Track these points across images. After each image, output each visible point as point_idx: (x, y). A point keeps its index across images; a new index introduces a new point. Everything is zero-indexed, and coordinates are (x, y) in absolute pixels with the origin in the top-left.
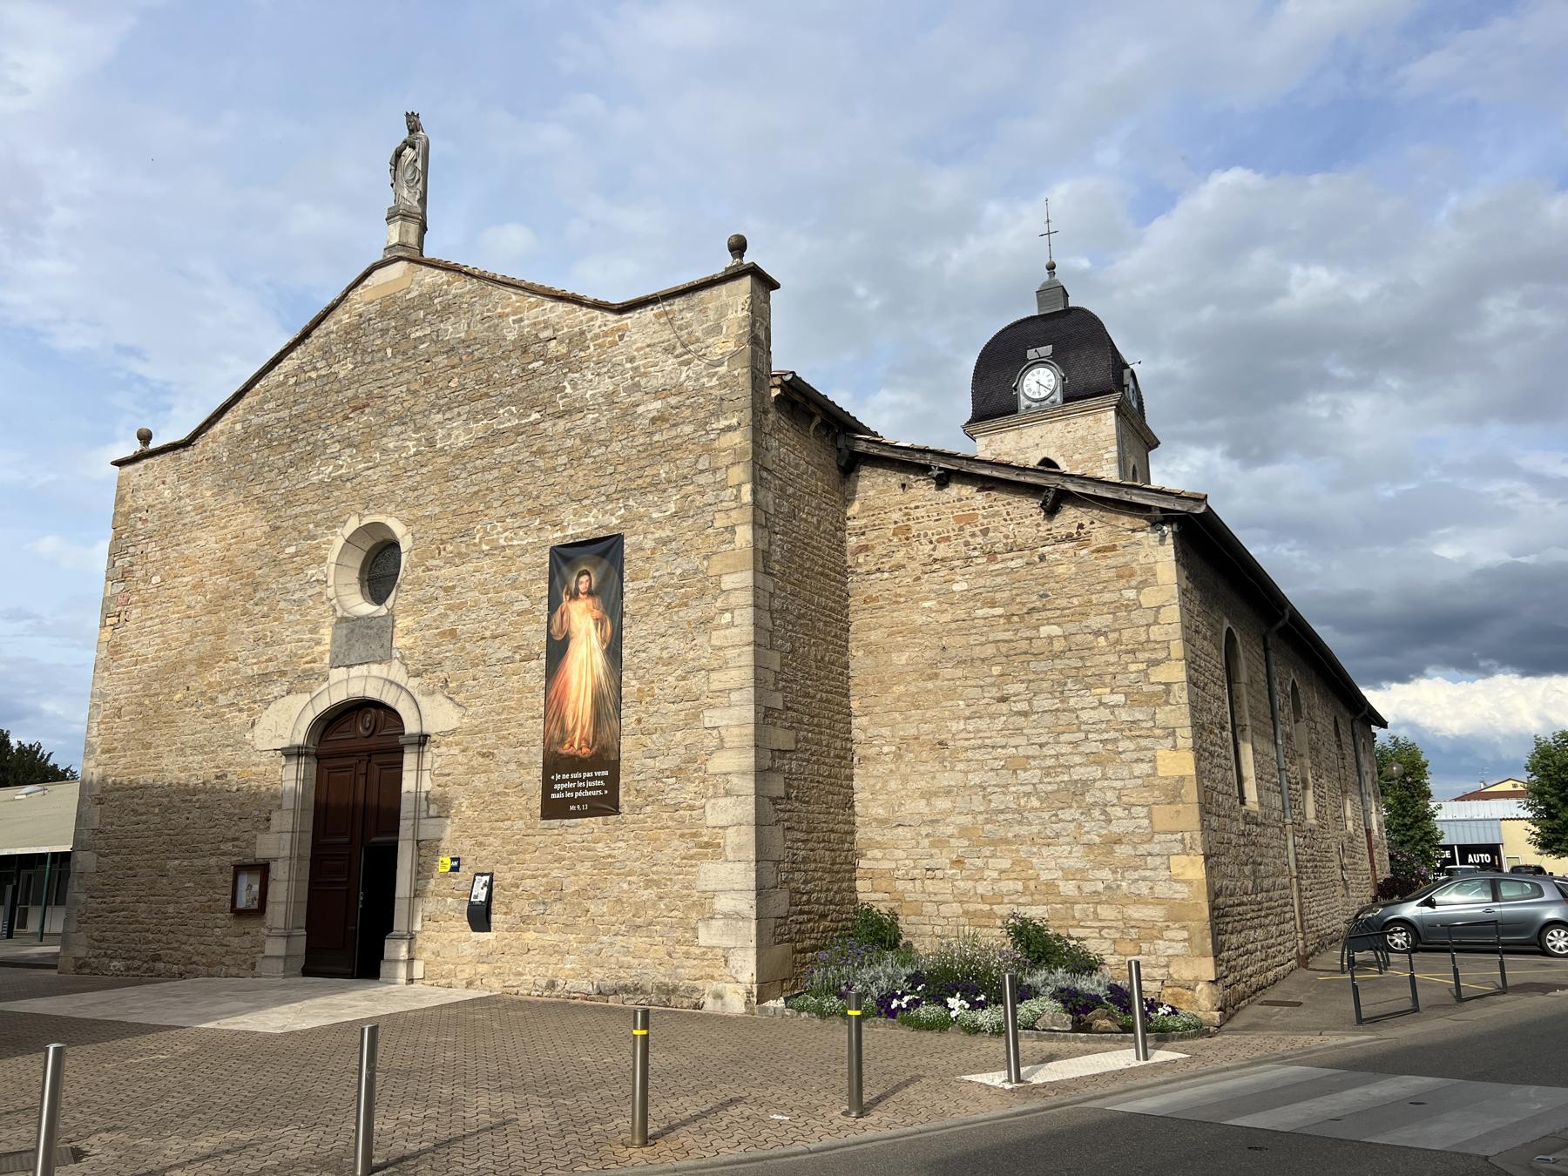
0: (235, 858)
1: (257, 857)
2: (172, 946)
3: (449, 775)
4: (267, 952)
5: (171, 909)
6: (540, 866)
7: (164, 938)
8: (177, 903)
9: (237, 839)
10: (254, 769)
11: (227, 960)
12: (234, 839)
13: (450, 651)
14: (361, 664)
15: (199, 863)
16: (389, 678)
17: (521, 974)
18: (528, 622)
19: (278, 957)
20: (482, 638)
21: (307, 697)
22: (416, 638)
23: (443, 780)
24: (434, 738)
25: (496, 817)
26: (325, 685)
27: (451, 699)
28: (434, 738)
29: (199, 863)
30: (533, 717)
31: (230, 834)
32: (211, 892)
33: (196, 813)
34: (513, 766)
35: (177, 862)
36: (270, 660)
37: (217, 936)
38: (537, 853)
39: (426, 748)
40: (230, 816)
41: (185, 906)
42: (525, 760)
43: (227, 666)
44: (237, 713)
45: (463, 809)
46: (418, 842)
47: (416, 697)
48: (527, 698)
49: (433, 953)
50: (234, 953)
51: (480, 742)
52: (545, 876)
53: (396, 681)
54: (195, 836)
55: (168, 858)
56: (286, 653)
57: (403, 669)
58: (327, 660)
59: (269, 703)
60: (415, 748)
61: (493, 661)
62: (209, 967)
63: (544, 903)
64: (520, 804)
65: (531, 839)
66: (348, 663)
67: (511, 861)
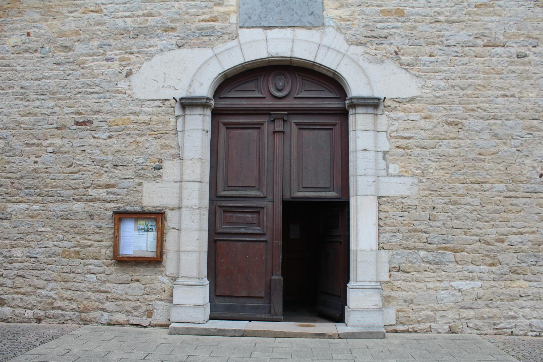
0: (112, 205)
1: (144, 205)
2: (22, 290)
3: (409, 138)
4: (176, 301)
5: (17, 253)
6: (526, 224)
7: (10, 283)
8: (26, 247)
9: (113, 186)
10: (132, 117)
11: (108, 305)
12: (108, 186)
13: (396, 28)
14: (282, 27)
15: (58, 208)
16: (323, 43)
17: (514, 318)
18: (488, 14)
19: (196, 306)
20: (437, 21)
21: (208, 52)
22: (354, 12)
23: (403, 142)
24: (387, 103)
25: (472, 180)
26: (234, 43)
27: (405, 69)
28: (387, 103)
29: (58, 208)
30: (505, 96)
31: (104, 180)
32: (78, 238)
33: (46, 157)
34: (486, 135)
35: (22, 206)
36: (150, 15)
37: (90, 282)
38: (522, 213)
39: (379, 112)
40: (101, 164)
41: (40, 250)
42: (500, 131)
43: (86, 16)
44: (105, 62)
45: (431, 171)
46: (379, 198)
47: (361, 63)
48: (495, 78)
49: (405, 301)
50: (117, 299)
51: (445, 112)
52: (533, 232)
53: (332, 46)
54: (48, 181)
55: (10, 201)
56: (173, 10)
57: (341, 37)
58: (233, 19)
59: (152, 55)
60: (370, 110)
61: (451, 42)
62: (82, 312)
63: (535, 256)
64: (499, 170)
65: (514, 201)
66: (266, 24)
67: (493, 219)
